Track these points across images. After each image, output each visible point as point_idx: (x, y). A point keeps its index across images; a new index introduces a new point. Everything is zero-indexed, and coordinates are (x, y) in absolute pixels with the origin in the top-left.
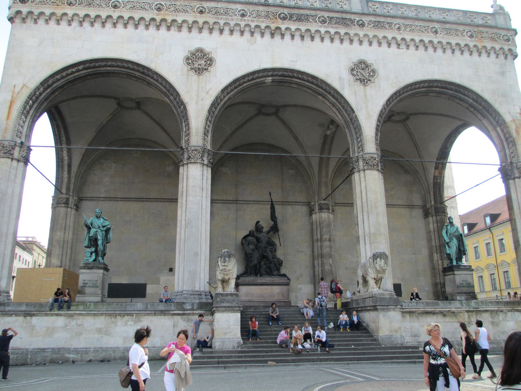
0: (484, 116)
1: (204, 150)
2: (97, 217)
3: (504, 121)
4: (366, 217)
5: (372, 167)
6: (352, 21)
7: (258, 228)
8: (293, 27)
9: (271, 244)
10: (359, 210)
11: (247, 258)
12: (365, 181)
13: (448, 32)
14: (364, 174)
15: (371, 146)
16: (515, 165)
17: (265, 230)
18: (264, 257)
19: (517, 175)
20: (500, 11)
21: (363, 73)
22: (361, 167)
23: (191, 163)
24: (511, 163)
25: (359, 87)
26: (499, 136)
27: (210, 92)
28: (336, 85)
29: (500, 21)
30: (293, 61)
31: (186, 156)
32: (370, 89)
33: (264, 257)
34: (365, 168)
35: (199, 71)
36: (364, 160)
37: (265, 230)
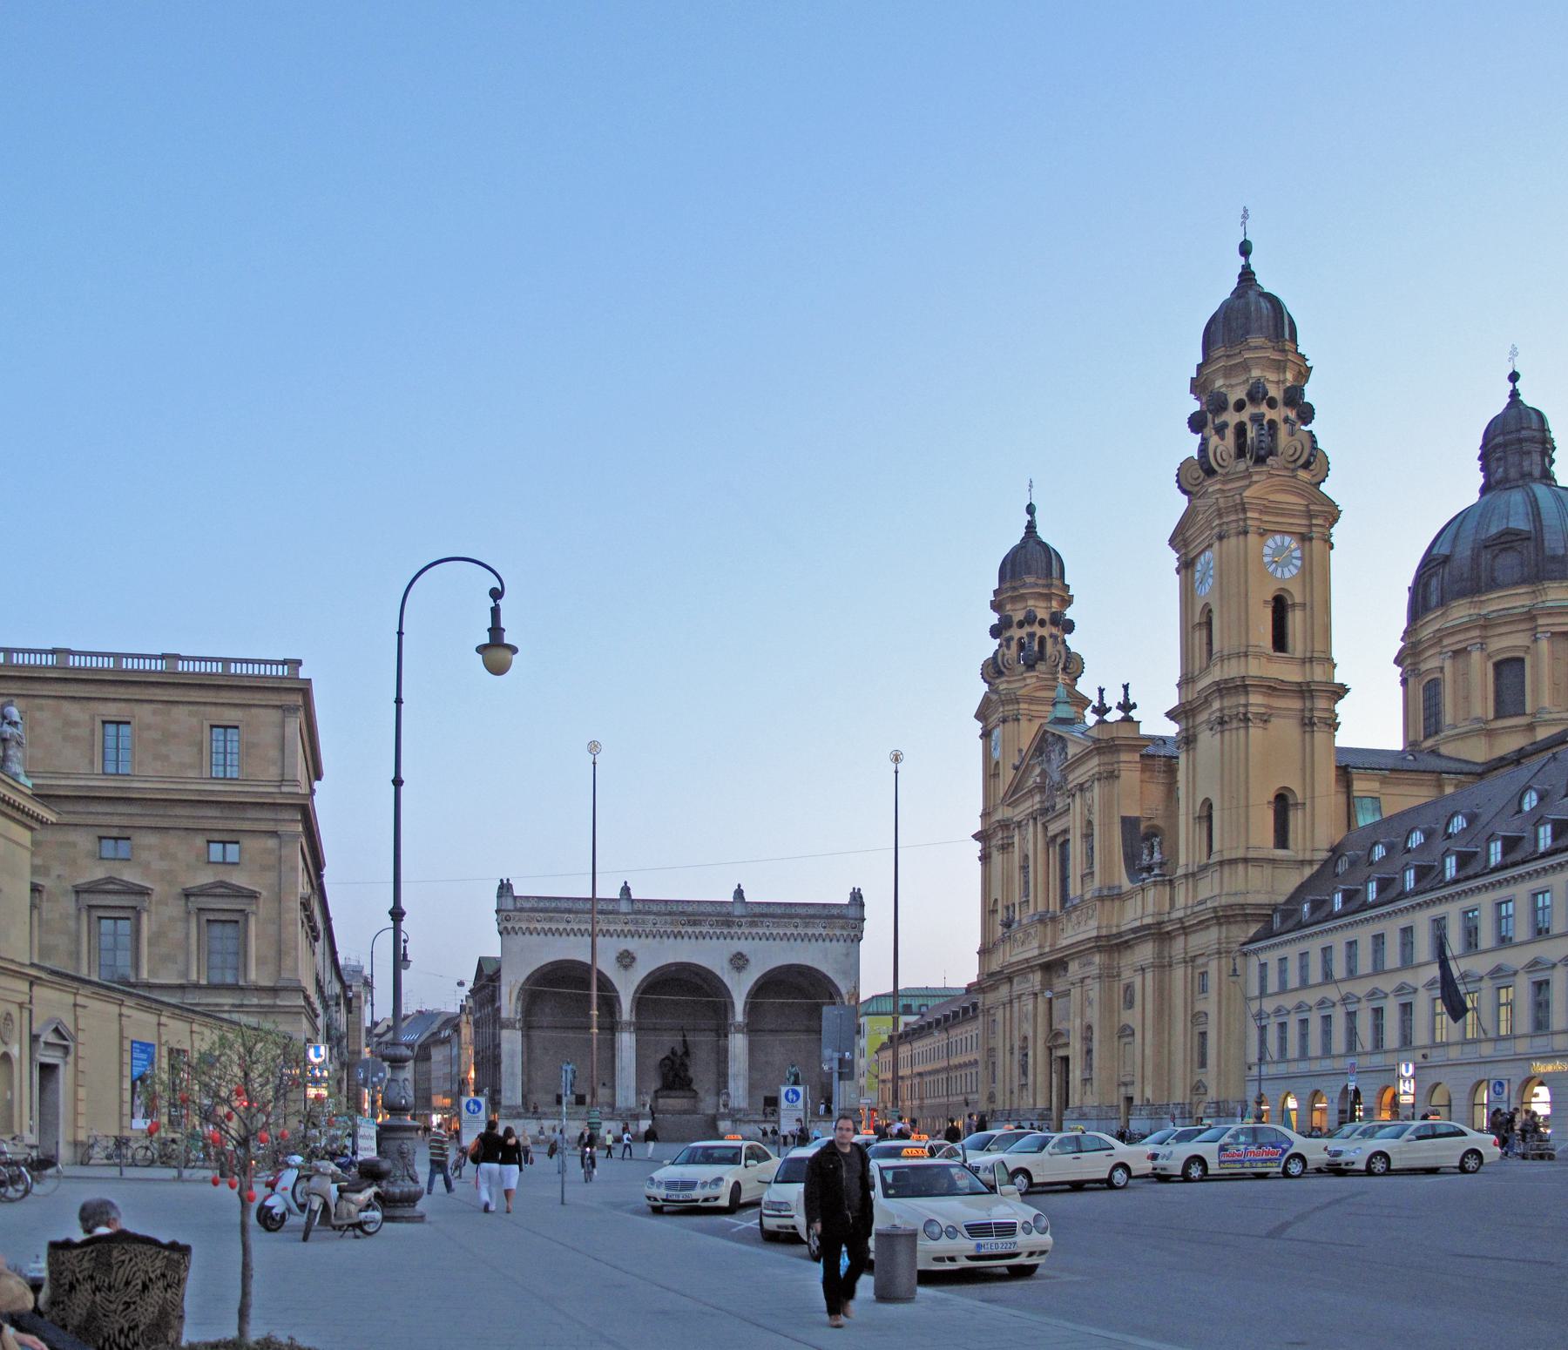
1: (630, 1024)
5: (738, 1031)
7: (673, 1052)
8: (690, 930)
9: (684, 1067)
11: (664, 1077)
13: (806, 925)
15: (739, 1016)
17: (679, 1053)
18: (676, 1075)
20: (857, 898)
21: (739, 962)
25: (735, 974)
28: (719, 973)
29: (852, 912)
32: (744, 975)
33: (676, 1075)
35: (626, 967)
37: (679, 1053)
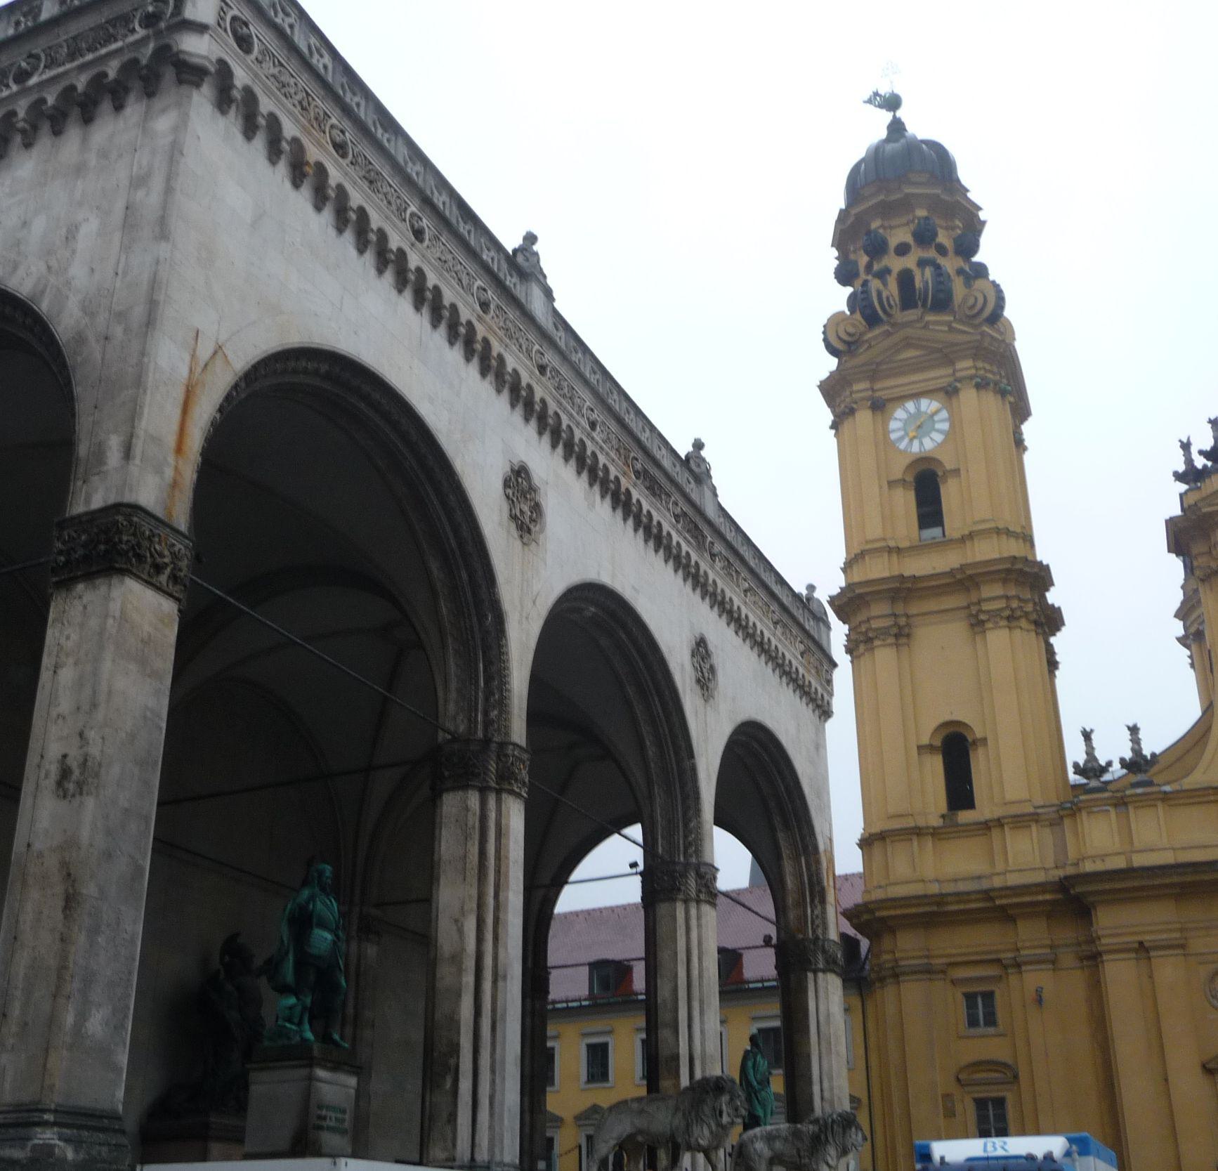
0: (787, 826)
2: (323, 889)
3: (816, 848)
4: (696, 1013)
6: (704, 537)
10: (682, 993)
12: (699, 926)
14: (698, 909)
16: (820, 943)
19: (821, 966)
22: (693, 894)
23: (511, 792)
24: (817, 938)
26: (801, 875)
27: (538, 603)
30: (636, 590)
31: (492, 767)
34: (702, 896)
36: (700, 876)
